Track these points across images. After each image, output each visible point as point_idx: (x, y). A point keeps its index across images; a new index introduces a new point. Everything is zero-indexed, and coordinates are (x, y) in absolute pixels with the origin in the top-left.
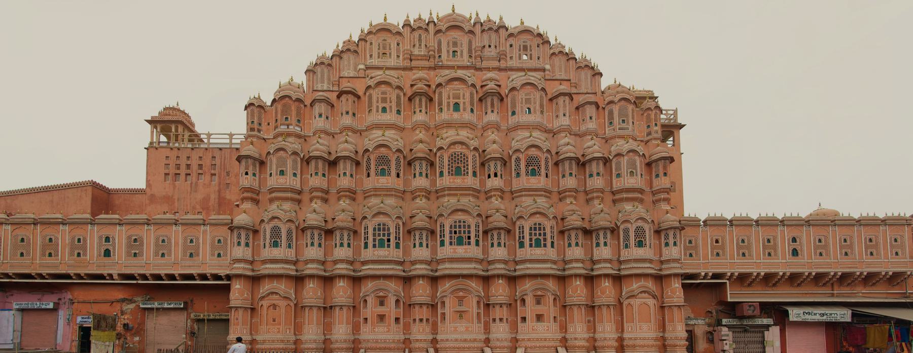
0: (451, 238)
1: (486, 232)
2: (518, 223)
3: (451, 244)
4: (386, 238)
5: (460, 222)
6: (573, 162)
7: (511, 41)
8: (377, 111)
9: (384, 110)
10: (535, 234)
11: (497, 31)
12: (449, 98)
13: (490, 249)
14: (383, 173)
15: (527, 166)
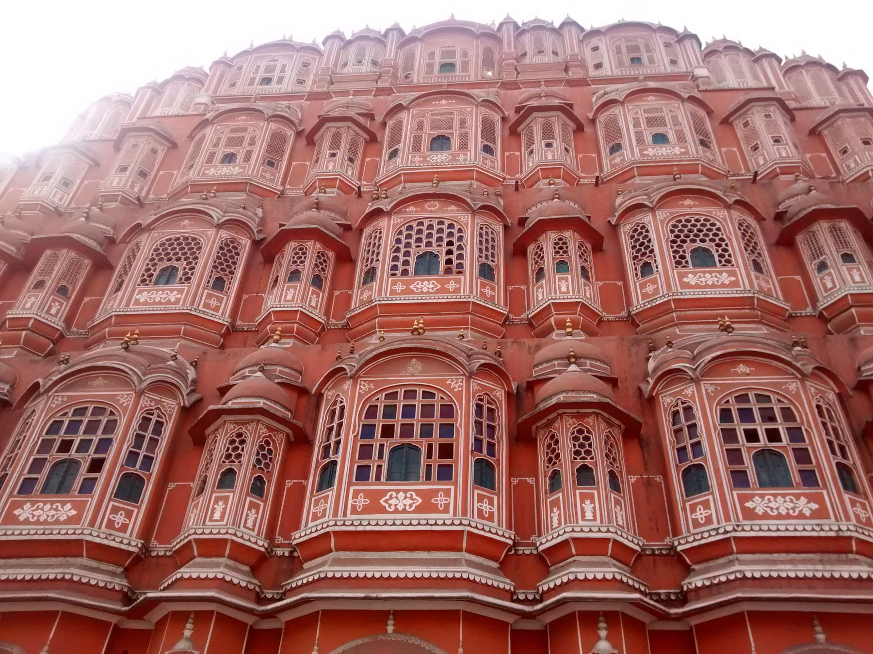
0: (365, 451)
1: (523, 438)
2: (666, 400)
3: (362, 474)
4: (91, 453)
5: (410, 394)
6: (844, 225)
7: (595, 41)
8: (210, 160)
9: (229, 158)
10: (752, 436)
11: (557, 32)
12: (420, 126)
13: (546, 501)
14: (168, 275)
15: (677, 241)
